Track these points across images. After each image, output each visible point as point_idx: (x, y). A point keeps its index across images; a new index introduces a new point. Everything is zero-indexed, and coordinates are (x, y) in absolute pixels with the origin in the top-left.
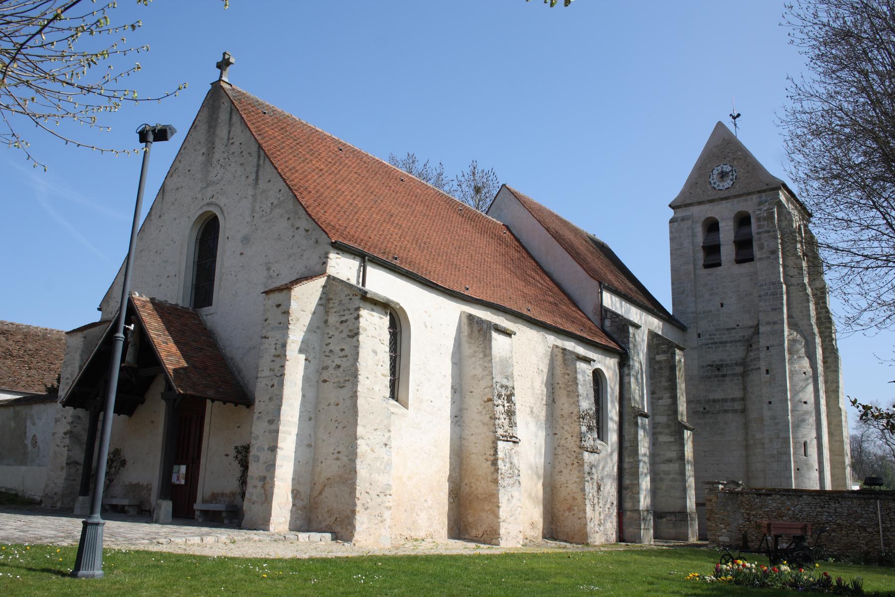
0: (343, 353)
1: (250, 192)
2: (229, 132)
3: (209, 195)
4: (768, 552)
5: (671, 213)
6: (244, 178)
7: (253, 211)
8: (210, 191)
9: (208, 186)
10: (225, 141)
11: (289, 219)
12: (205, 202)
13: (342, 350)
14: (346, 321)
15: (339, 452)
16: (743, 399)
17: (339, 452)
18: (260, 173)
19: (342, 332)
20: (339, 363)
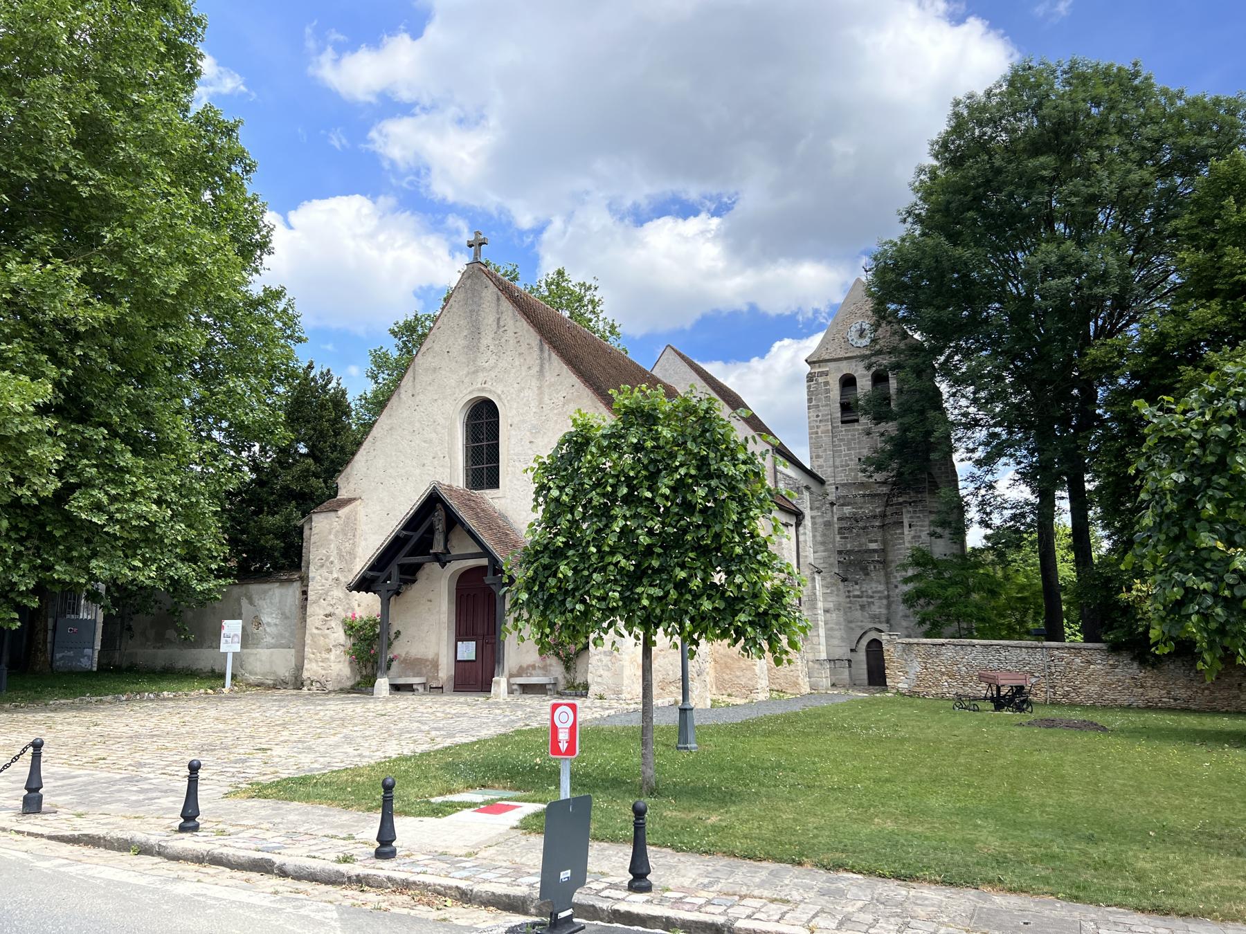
1: (535, 383)
3: (480, 380)
4: (992, 699)
5: (808, 368)
6: (524, 368)
7: (541, 402)
8: (481, 377)
9: (475, 372)
10: (494, 326)
12: (474, 387)
16: (883, 550)
18: (547, 366)
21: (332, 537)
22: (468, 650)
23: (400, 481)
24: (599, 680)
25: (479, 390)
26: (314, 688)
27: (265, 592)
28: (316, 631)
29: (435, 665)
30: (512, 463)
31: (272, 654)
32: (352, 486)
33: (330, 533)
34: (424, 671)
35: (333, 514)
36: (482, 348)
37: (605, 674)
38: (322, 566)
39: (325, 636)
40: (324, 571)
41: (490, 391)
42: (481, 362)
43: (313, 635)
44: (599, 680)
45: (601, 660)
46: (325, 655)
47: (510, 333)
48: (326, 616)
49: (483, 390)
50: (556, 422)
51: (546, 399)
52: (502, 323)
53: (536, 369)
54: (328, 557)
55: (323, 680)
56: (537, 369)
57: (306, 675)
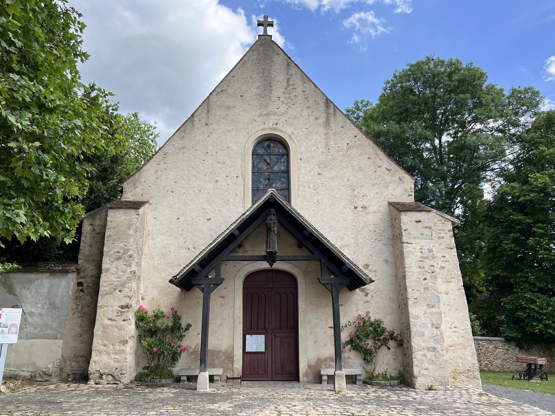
0: (445, 258)
1: (322, 130)
2: (288, 80)
3: (272, 122)
6: (312, 119)
7: (327, 145)
8: (272, 119)
10: (285, 84)
11: (369, 158)
12: (266, 126)
13: (444, 257)
14: (443, 238)
15: (455, 327)
17: (455, 327)
18: (332, 119)
19: (440, 245)
20: (443, 265)
21: (131, 232)
22: (257, 343)
23: (191, 191)
24: (426, 372)
25: (271, 129)
26: (104, 381)
27: (30, 281)
28: (109, 323)
29: (230, 357)
30: (302, 188)
31: (32, 345)
32: (139, 190)
33: (129, 228)
34: (217, 362)
35: (133, 211)
36: (274, 98)
37: (431, 367)
38: (119, 259)
39: (120, 328)
40: (121, 264)
41: (282, 131)
42: (272, 107)
43: (105, 327)
44: (426, 372)
45: (424, 355)
46: (118, 347)
47: (299, 91)
48: (122, 307)
49: (275, 129)
50: (342, 161)
51: (332, 143)
52: (291, 82)
53: (322, 120)
54: (126, 251)
55: (116, 373)
56: (324, 120)
57: (92, 367)
